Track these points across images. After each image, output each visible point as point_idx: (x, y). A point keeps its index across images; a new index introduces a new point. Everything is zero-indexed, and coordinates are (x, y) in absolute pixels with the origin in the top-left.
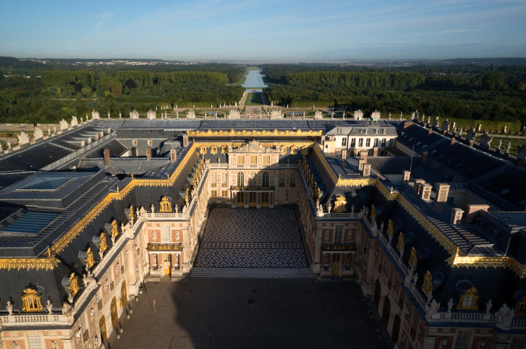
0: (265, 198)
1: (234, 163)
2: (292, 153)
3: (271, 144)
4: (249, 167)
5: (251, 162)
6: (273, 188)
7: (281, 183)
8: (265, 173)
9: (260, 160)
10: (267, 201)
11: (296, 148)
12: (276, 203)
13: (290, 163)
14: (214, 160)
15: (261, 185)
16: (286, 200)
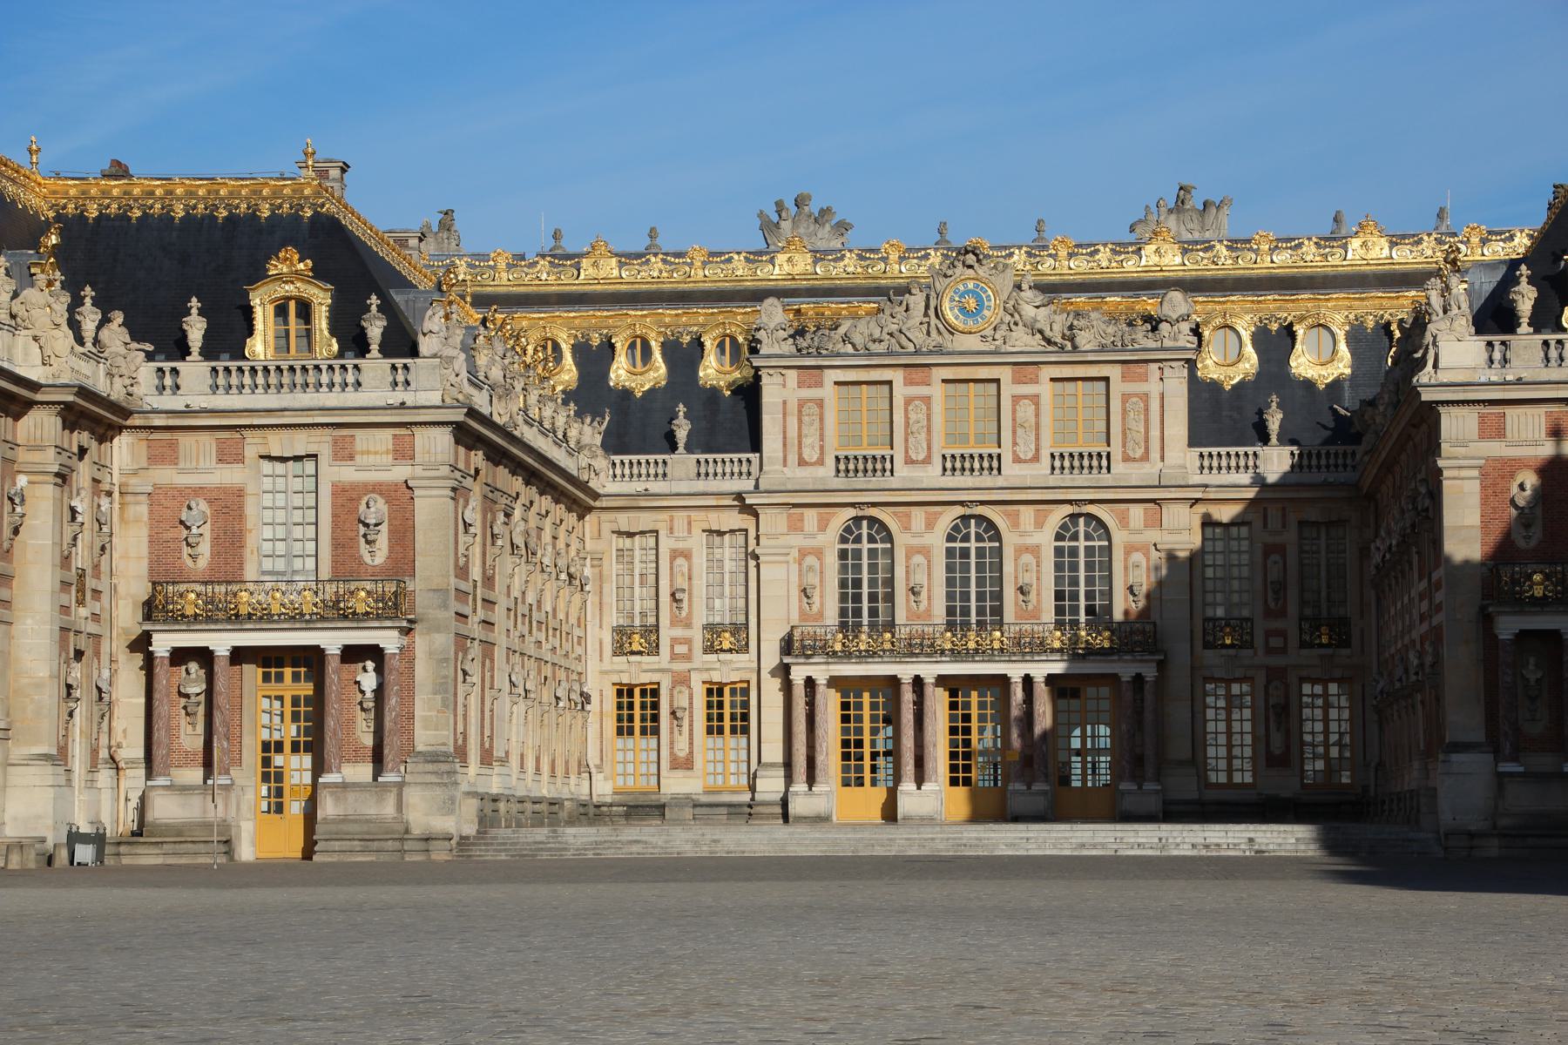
1: (811, 440)
9: (1026, 411)
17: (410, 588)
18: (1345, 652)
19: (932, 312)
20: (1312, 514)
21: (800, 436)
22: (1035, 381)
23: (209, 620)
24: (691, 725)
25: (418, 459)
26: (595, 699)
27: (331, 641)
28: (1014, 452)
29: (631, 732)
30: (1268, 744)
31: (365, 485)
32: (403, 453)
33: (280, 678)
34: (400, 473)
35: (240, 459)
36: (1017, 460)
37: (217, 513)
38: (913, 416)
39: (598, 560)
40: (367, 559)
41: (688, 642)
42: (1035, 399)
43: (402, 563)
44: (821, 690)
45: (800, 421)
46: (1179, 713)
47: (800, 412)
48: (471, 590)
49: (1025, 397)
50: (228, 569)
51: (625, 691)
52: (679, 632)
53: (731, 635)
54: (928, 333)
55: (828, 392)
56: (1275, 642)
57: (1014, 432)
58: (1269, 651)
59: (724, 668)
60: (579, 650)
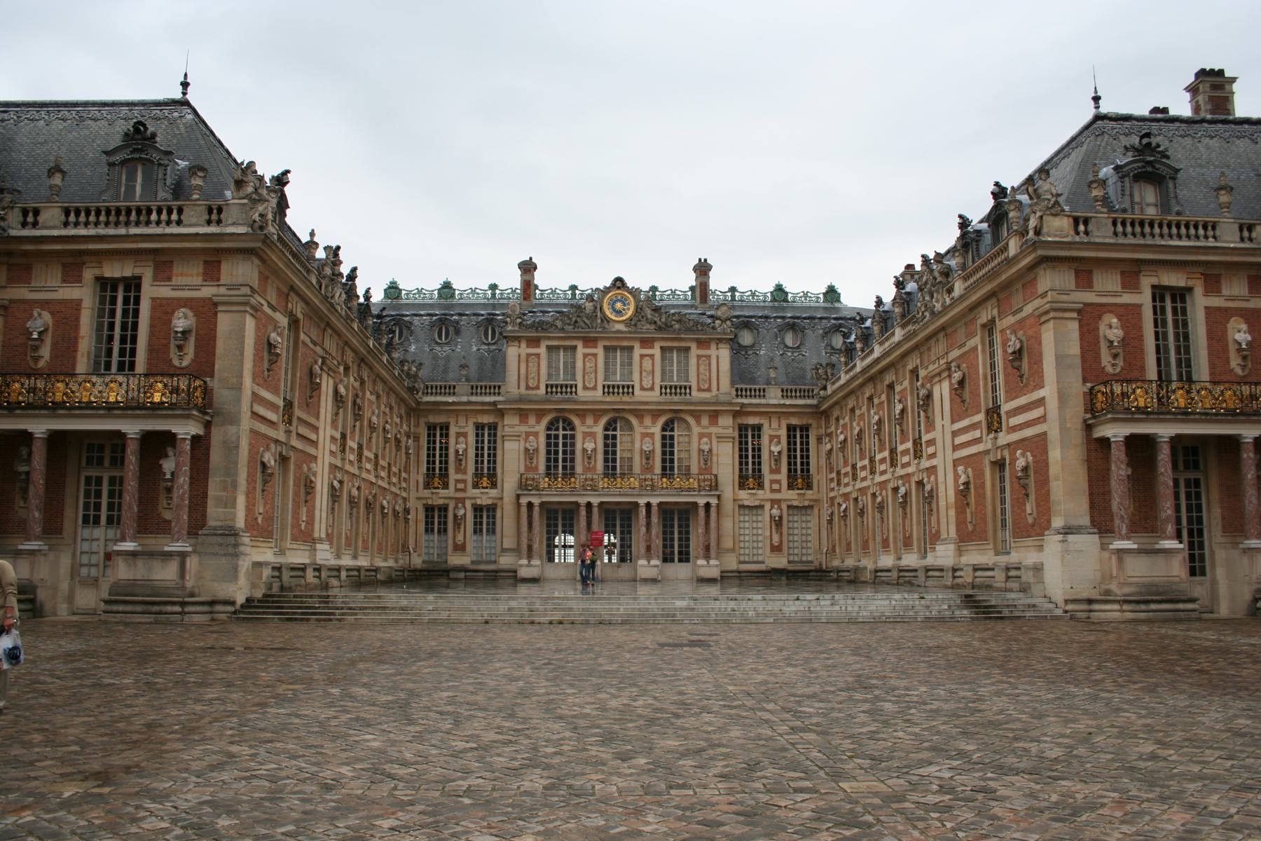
9: (647, 363)
17: (210, 384)
20: (794, 421)
22: (652, 347)
23: (30, 406)
25: (222, 282)
26: (413, 512)
27: (132, 428)
29: (433, 530)
31: (179, 299)
32: (212, 272)
33: (100, 462)
34: (207, 292)
35: (79, 279)
36: (642, 389)
37: (57, 324)
38: (588, 365)
39: (417, 439)
40: (176, 362)
41: (464, 481)
42: (652, 356)
43: (204, 366)
44: (536, 510)
46: (727, 524)
48: (281, 403)
50: (63, 368)
51: (429, 509)
52: (459, 477)
55: (542, 350)
56: (776, 486)
59: (484, 497)
60: (404, 485)
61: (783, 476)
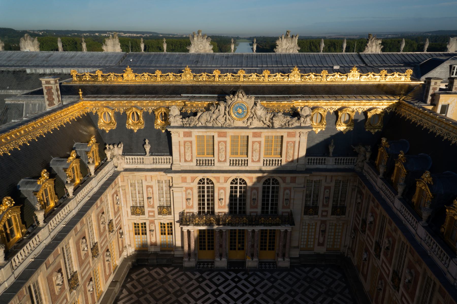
0: (267, 241)
2: (342, 128)
3: (286, 104)
4: (226, 166)
5: (234, 153)
6: (289, 219)
7: (310, 203)
8: (271, 183)
9: (257, 146)
10: (272, 248)
11: (353, 115)
12: (295, 253)
13: (335, 154)
14: (133, 146)
15: (259, 210)
16: (319, 244)
18: (344, 216)
19: (227, 113)
21: (185, 152)
24: (156, 234)
28: (252, 159)
30: (319, 240)
36: (253, 161)
38: (220, 147)
41: (153, 212)
45: (185, 148)
47: (184, 144)
49: (256, 142)
52: (150, 209)
53: (165, 209)
54: (226, 120)
56: (324, 214)
57: (252, 153)
58: (322, 216)
61: (330, 209)
